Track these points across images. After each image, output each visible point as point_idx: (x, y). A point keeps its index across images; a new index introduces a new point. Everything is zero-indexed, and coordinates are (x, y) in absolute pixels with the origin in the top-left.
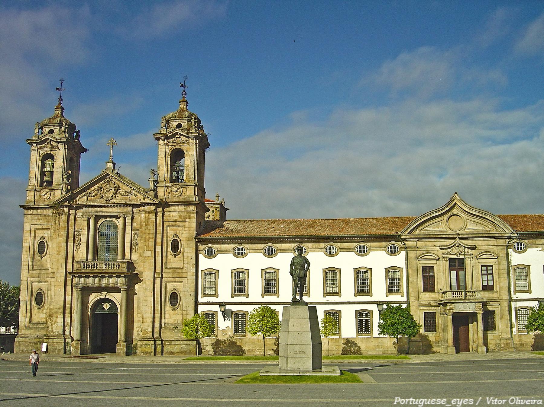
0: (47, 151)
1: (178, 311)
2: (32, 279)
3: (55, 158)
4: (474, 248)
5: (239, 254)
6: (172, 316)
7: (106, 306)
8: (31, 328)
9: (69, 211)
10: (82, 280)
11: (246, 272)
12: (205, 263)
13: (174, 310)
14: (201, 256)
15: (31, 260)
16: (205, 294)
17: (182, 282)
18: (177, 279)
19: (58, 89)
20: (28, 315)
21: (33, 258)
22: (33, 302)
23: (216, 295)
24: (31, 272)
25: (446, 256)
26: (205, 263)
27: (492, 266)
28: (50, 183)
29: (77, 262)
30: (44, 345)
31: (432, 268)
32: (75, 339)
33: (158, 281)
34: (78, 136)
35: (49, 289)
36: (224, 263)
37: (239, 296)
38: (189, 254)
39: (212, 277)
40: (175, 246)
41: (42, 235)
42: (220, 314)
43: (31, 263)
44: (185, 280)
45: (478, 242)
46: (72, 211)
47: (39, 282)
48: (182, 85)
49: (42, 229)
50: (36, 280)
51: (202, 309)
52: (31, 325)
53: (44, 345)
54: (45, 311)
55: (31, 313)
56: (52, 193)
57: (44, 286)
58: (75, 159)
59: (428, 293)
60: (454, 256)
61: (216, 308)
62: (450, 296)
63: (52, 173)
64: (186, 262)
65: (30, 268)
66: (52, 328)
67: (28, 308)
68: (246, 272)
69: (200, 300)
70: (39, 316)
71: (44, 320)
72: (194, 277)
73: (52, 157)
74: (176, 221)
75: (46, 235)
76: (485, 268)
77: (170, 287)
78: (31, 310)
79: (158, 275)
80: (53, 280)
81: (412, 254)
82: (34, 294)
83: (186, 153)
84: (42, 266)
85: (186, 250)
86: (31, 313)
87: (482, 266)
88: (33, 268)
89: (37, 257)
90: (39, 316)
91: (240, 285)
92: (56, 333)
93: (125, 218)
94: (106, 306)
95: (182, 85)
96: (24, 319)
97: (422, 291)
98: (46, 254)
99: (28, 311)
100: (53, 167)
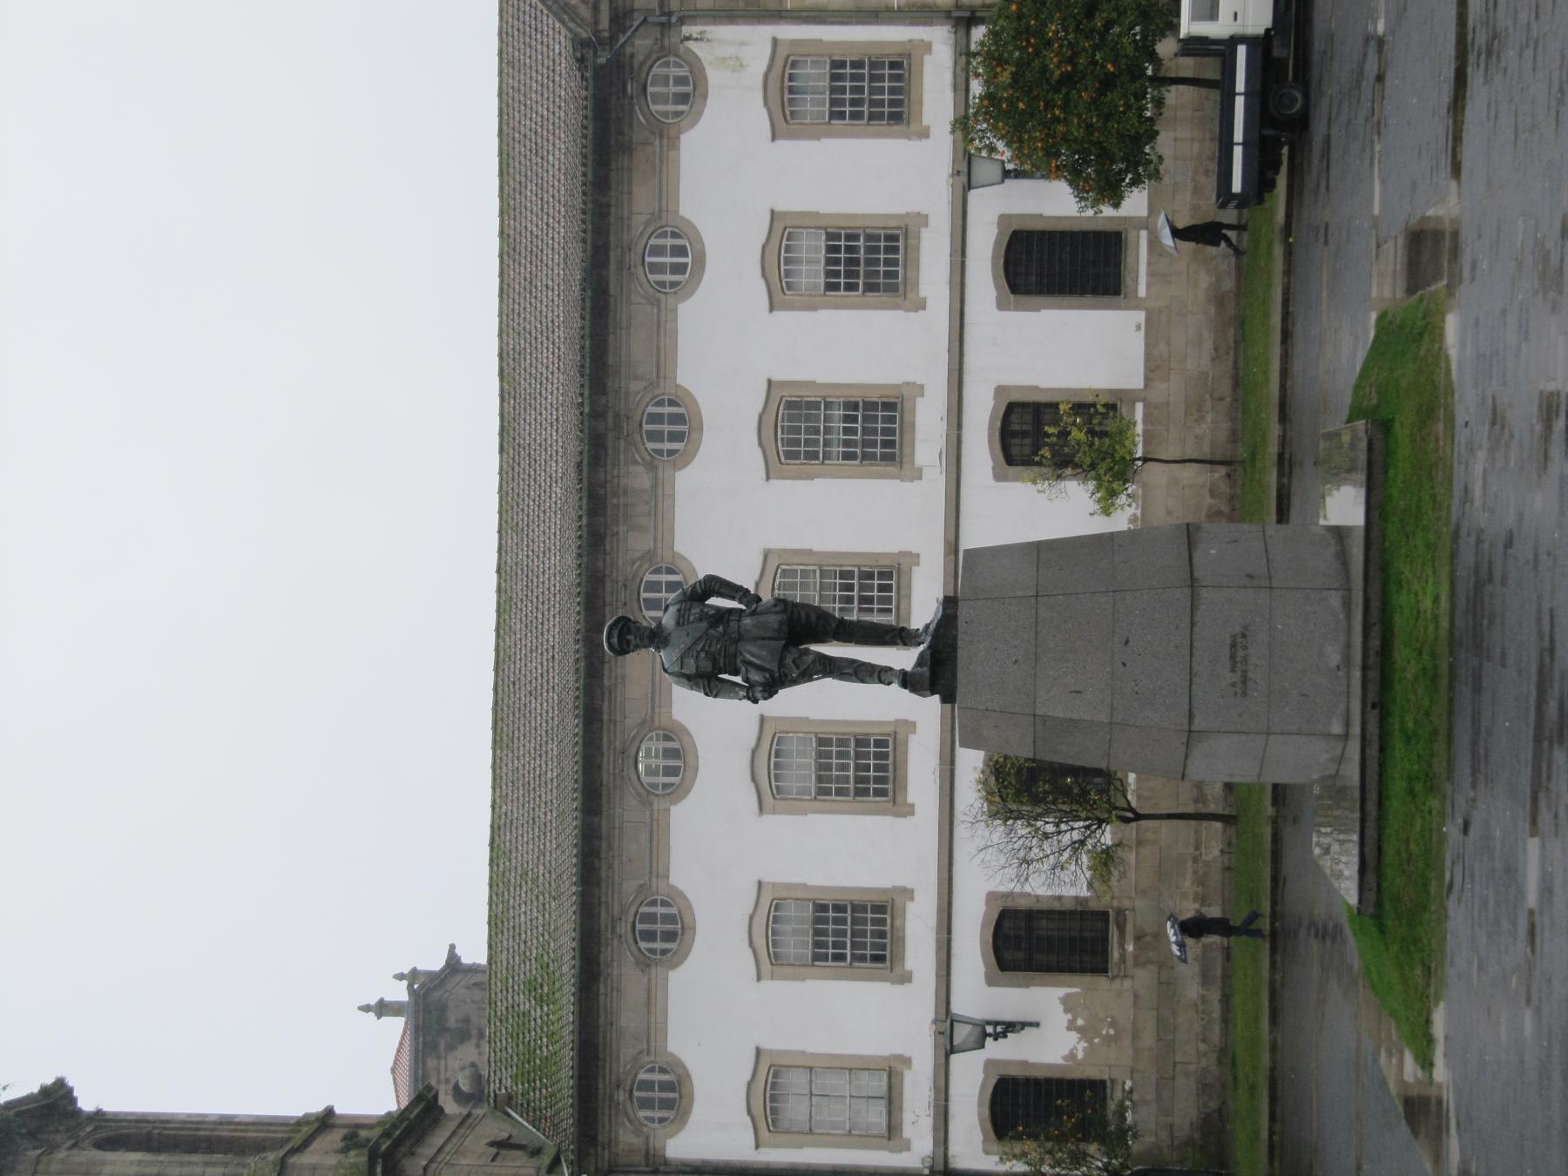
5: (669, 933)
16: (892, 1132)
23: (892, 1071)
36: (719, 1018)
37: (899, 941)
39: (796, 1082)
42: (997, 1050)
91: (851, 934)
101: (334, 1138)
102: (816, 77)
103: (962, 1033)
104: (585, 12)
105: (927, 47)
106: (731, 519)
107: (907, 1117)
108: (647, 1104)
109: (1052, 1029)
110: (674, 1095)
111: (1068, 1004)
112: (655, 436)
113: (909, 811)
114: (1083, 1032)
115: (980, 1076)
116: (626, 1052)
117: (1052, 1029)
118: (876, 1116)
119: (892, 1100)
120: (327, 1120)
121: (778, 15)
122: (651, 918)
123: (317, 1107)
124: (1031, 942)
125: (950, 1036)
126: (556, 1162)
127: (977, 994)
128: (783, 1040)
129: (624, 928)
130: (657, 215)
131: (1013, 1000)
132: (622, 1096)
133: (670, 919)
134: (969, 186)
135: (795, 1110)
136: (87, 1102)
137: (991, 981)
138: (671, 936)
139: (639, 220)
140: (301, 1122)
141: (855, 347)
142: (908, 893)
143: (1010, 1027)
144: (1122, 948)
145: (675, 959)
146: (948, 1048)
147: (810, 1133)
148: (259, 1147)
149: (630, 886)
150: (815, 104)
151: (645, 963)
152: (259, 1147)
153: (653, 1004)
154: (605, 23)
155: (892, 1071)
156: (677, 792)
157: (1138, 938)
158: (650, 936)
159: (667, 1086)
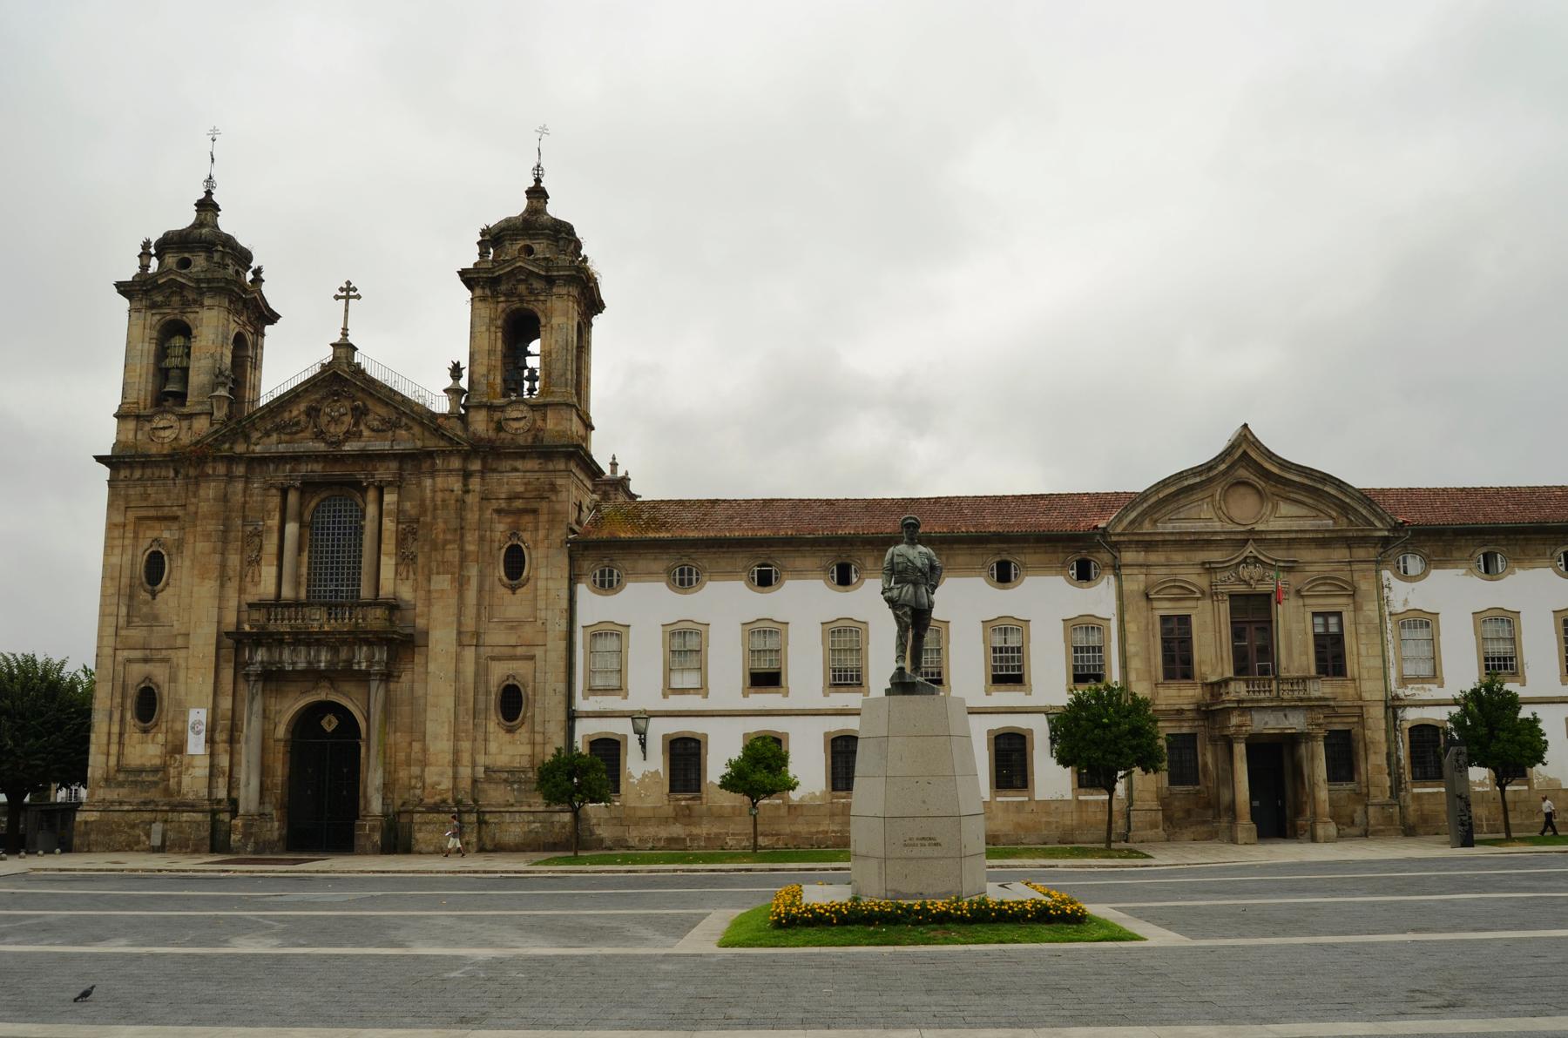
0: (171, 313)
1: (523, 734)
2: (126, 654)
3: (194, 332)
4: (1291, 567)
5: (684, 581)
7: (330, 723)
8: (121, 785)
9: (229, 470)
10: (261, 655)
12: (592, 606)
13: (510, 731)
14: (582, 590)
15: (124, 601)
16: (592, 691)
17: (532, 658)
18: (520, 651)
20: (114, 749)
21: (131, 597)
22: (129, 715)
23: (620, 690)
24: (123, 632)
25: (1220, 589)
27: (1339, 614)
28: (181, 397)
29: (250, 605)
30: (157, 828)
31: (1185, 620)
32: (241, 811)
33: (469, 654)
34: (258, 279)
35: (173, 679)
36: (643, 606)
38: (551, 584)
39: (612, 644)
40: (515, 563)
41: (155, 534)
42: (633, 740)
43: (123, 610)
44: (538, 652)
45: (1304, 555)
46: (240, 470)
47: (146, 660)
49: (158, 519)
50: (138, 654)
52: (121, 777)
53: (157, 828)
54: (161, 738)
55: (121, 743)
56: (185, 424)
57: (159, 673)
58: (249, 338)
59: (1174, 684)
60: (1242, 588)
61: (621, 728)
62: (1238, 690)
63: (185, 370)
64: (541, 604)
65: (122, 621)
66: (179, 783)
67: (115, 729)
69: (581, 704)
70: (145, 751)
71: (157, 762)
72: (563, 644)
73: (185, 331)
76: (1319, 620)
77: (499, 673)
78: (121, 735)
79: (469, 638)
80: (182, 653)
81: (1135, 583)
82: (132, 693)
83: (543, 321)
84: (156, 618)
85: (542, 573)
86: (121, 743)
87: (1315, 614)
88: (129, 623)
89: (146, 596)
90: (145, 751)
92: (191, 796)
94: (330, 723)
96: (103, 758)
97: (1161, 680)
98: (167, 584)
99: (115, 739)
100: (188, 355)
101: (582, 431)
102: (1094, 640)
103: (641, 723)
104: (1119, 530)
106: (964, 602)
107: (599, 698)
108: (602, 573)
109: (644, 767)
110: (607, 584)
111: (657, 772)
114: (641, 781)
116: (627, 564)
117: (644, 767)
118: (599, 682)
119: (606, 691)
120: (589, 427)
121: (1122, 622)
122: (690, 573)
123: (594, 423)
124: (685, 756)
125: (640, 719)
126: (574, 532)
127: (659, 730)
129: (685, 560)
130: (1024, 565)
132: (606, 562)
133: (690, 582)
134: (1047, 714)
135: (601, 644)
136: (597, 321)
137: (664, 736)
138: (682, 583)
139: (1022, 558)
140: (588, 415)
143: (643, 745)
144: (683, 800)
145: (671, 585)
146: (633, 716)
147: (591, 652)
148: (578, 394)
149: (705, 563)
150: (1081, 639)
151: (669, 571)
152: (578, 394)
153: (650, 575)
154: (1114, 539)
155: (620, 690)
157: (688, 807)
158: (682, 572)
159: (611, 583)
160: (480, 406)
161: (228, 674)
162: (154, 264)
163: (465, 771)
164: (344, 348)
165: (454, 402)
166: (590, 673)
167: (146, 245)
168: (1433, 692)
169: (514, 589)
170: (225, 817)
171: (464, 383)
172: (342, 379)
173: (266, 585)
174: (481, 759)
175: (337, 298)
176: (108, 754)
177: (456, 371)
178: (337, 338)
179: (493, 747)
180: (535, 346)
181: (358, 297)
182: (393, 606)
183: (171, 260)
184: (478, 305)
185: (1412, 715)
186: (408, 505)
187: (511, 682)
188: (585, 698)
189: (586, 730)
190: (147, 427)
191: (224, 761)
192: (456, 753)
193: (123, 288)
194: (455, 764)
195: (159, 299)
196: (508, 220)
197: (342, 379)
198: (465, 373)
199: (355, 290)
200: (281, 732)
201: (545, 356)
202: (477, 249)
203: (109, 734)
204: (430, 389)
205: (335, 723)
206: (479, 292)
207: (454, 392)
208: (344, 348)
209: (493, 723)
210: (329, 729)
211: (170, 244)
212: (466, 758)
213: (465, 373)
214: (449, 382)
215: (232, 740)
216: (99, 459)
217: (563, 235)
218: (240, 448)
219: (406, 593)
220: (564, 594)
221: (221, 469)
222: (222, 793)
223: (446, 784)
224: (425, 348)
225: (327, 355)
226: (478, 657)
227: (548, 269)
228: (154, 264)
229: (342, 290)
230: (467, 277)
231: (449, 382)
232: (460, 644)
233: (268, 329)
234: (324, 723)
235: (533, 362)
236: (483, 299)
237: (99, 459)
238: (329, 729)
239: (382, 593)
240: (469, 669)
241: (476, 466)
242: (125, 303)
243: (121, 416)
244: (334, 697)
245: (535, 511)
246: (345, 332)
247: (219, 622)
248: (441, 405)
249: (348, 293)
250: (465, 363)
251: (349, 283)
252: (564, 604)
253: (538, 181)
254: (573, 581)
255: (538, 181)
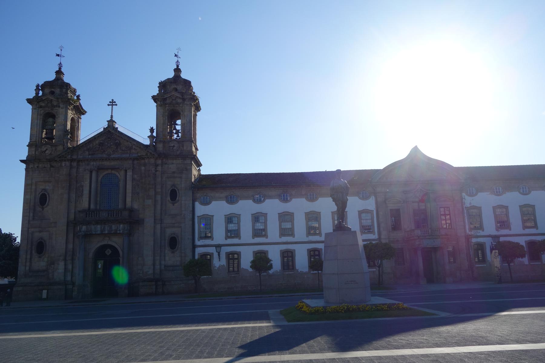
2: (32, 230)
3: (57, 116)
5: (231, 201)
6: (172, 259)
7: (108, 252)
11: (238, 216)
12: (200, 210)
13: (173, 252)
14: (197, 204)
16: (201, 238)
19: (58, 55)
20: (28, 264)
22: (34, 252)
23: (211, 238)
26: (200, 210)
29: (79, 212)
30: (45, 292)
33: (158, 226)
36: (217, 209)
42: (216, 255)
43: (31, 215)
46: (75, 164)
47: (40, 232)
48: (176, 56)
51: (199, 251)
53: (45, 292)
54: (46, 259)
56: (54, 148)
61: (212, 250)
67: (29, 257)
68: (238, 216)
69: (198, 243)
70: (40, 264)
72: (191, 222)
73: (53, 116)
74: (174, 173)
75: (47, 188)
77: (169, 232)
78: (31, 259)
83: (182, 113)
88: (34, 219)
90: (40, 264)
93: (126, 171)
95: (176, 56)
98: (48, 205)
105: (374, 235)
107: (203, 240)
109: (219, 262)
112: (310, 195)
113: (253, 238)
115: (211, 252)
119: (206, 237)
125: (218, 247)
128: (242, 218)
131: (223, 256)
141: (300, 226)
142: (240, 239)
153: (220, 199)
155: (211, 238)
156: (254, 201)
160: (160, 141)
161: (71, 236)
162: (41, 93)
163: (158, 267)
164: (111, 122)
165: (151, 142)
166: (200, 232)
167: (38, 86)
168: (481, 233)
169: (173, 204)
170: (70, 287)
171: (155, 134)
172: (111, 134)
173: (85, 204)
174: (163, 262)
175: (109, 105)
176: (26, 266)
177: (152, 130)
178: (109, 119)
179: (167, 258)
180: (179, 122)
181: (116, 105)
182: (131, 211)
183: (47, 91)
184: (159, 108)
185: (474, 240)
186: (136, 176)
187: (173, 236)
188: (199, 241)
189: (199, 251)
190: (40, 150)
191: (70, 267)
192: (154, 260)
193: (29, 101)
194: (154, 265)
195: (43, 105)
196: (168, 79)
197: (111, 134)
198: (155, 131)
199: (115, 102)
200: (91, 255)
201: (182, 125)
202: (158, 89)
203: (26, 259)
204: (143, 137)
205: (110, 252)
206: (159, 103)
207: (151, 137)
208: (111, 122)
209: (168, 251)
210: (108, 254)
211: (47, 85)
212: (157, 263)
213: (155, 131)
214: (150, 134)
215: (73, 259)
216: (22, 161)
217: (187, 84)
218: (75, 157)
219: (136, 206)
220: (191, 205)
221: (68, 163)
222: (69, 278)
223: (151, 272)
224: (140, 123)
225: (106, 125)
226: (161, 228)
227: (182, 96)
228: (41, 93)
229: (110, 102)
230: (154, 98)
231: (150, 134)
232: (155, 222)
233: (82, 116)
234: (106, 252)
235: (178, 128)
236: (161, 106)
237: (22, 161)
238: (108, 254)
239: (127, 206)
240: (158, 232)
241: (159, 162)
242: (30, 107)
243: (29, 146)
244: (110, 243)
245: (181, 177)
246: (112, 116)
247: (68, 218)
248: (147, 142)
249: (113, 103)
250: (155, 127)
251: (113, 100)
252: (191, 209)
253: (178, 66)
254: (194, 201)
255: (178, 66)
